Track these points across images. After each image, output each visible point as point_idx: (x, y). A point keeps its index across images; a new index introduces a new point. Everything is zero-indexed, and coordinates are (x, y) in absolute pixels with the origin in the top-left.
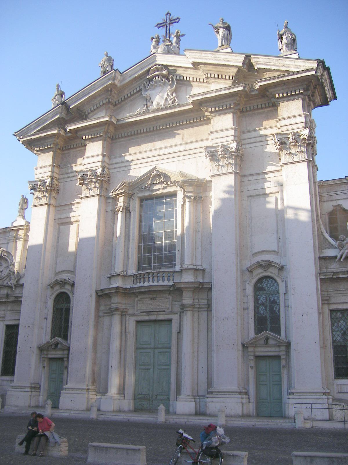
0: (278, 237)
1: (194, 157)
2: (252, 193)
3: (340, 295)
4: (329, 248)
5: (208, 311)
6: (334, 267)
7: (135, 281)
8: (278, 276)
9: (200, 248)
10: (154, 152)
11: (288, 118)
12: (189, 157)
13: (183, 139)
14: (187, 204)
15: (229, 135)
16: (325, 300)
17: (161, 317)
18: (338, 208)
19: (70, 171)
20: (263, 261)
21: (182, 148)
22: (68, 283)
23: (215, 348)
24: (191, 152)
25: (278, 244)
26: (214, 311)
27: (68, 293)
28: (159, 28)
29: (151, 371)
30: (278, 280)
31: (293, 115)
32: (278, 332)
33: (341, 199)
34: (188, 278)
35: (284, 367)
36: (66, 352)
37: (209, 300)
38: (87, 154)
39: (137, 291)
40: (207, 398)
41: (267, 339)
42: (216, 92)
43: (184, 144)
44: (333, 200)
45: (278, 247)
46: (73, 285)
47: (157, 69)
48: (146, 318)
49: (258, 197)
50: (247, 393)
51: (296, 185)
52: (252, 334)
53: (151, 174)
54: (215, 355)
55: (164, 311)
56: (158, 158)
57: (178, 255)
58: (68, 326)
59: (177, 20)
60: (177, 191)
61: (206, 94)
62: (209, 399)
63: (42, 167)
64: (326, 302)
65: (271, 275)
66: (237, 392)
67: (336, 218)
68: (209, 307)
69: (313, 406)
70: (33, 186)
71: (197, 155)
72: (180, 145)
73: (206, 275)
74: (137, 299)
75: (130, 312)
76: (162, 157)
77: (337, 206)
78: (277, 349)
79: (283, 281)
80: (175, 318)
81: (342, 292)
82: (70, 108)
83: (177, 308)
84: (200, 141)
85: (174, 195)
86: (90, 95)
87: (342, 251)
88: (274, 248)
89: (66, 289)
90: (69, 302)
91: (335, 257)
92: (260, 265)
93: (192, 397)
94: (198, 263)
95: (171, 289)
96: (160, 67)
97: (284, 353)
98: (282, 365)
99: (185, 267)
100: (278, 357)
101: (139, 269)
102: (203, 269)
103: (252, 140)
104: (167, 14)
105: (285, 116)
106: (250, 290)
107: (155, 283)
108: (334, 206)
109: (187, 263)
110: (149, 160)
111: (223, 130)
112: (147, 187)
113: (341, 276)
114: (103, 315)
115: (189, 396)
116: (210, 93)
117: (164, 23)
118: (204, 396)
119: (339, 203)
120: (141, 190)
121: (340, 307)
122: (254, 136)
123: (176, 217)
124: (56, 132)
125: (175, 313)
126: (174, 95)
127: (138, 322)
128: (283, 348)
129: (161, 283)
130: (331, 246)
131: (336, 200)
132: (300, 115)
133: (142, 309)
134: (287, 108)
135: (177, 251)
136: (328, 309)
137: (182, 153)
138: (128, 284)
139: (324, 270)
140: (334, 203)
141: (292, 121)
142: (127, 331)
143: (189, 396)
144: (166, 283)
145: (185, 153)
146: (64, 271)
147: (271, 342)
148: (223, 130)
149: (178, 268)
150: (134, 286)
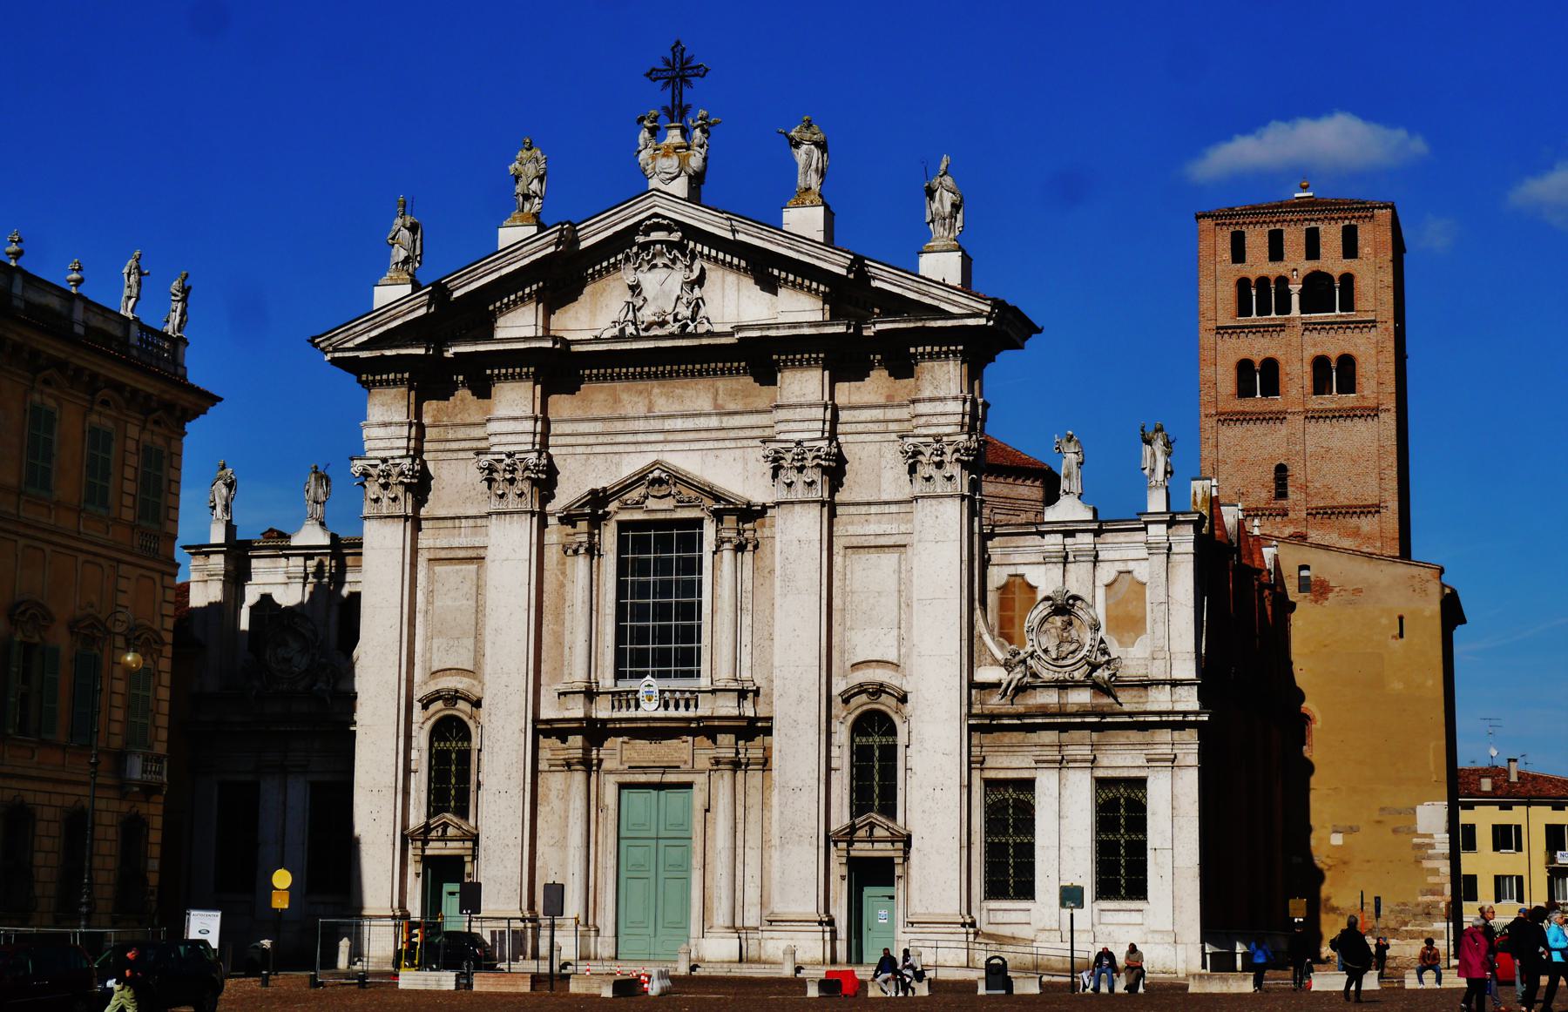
0: (899, 636)
1: (739, 445)
2: (855, 542)
3: (1003, 753)
4: (992, 665)
5: (764, 771)
6: (995, 702)
7: (616, 704)
8: (897, 713)
9: (749, 646)
10: (652, 421)
11: (931, 400)
12: (728, 444)
13: (715, 399)
14: (727, 555)
15: (813, 417)
16: (974, 763)
17: (671, 778)
18: (1018, 580)
19: (450, 437)
20: (871, 684)
21: (714, 422)
22: (466, 699)
23: (776, 841)
24: (732, 434)
25: (899, 650)
26: (775, 773)
27: (466, 718)
28: (654, 80)
29: (653, 880)
30: (897, 719)
31: (942, 394)
32: (892, 815)
33: (1024, 564)
34: (727, 707)
35: (899, 877)
36: (469, 844)
37: (767, 750)
38: (500, 411)
39: (623, 725)
40: (762, 931)
41: (872, 826)
42: (789, 328)
43: (717, 414)
44: (1010, 565)
45: (899, 655)
46: (477, 704)
47: (658, 227)
48: (642, 778)
49: (866, 549)
50: (831, 922)
51: (937, 542)
52: (841, 818)
53: (646, 475)
54: (776, 855)
55: (678, 767)
56: (661, 437)
57: (705, 656)
58: (469, 788)
59: (701, 72)
60: (702, 519)
61: (769, 329)
62: (766, 934)
63: (385, 425)
64: (978, 766)
65: (883, 708)
66: (815, 921)
67: (1013, 599)
68: (765, 764)
69: (940, 944)
70: (364, 469)
71: (745, 443)
72: (709, 415)
73: (761, 698)
74: (621, 739)
75: (606, 765)
76: (670, 437)
77: (1016, 575)
78: (889, 846)
79: (905, 722)
80: (700, 780)
81: (1006, 749)
82: (457, 294)
83: (703, 761)
84: (751, 412)
85: (698, 523)
86: (504, 272)
87: (1011, 675)
88: (892, 657)
89: (456, 709)
90: (467, 736)
91: (998, 685)
92: (861, 689)
93: (733, 931)
94: (746, 674)
95: (693, 725)
96: (665, 222)
97: (901, 854)
98: (896, 874)
99: (720, 685)
100: (888, 863)
101: (619, 675)
102: (755, 688)
103: (860, 428)
104: (673, 49)
105: (927, 394)
106: (842, 735)
107: (661, 713)
108: (1011, 576)
109: (724, 675)
110: (640, 438)
111: (801, 406)
112: (638, 503)
113: (1006, 722)
114: (547, 768)
115: (728, 928)
116: (778, 328)
117: (664, 71)
118: (757, 929)
119: (1020, 570)
120: (625, 507)
121: (1001, 775)
122: (862, 418)
123: (700, 573)
124: (422, 351)
125: (701, 772)
126: (697, 292)
127: (622, 786)
128: (900, 845)
129: (671, 712)
130: (995, 662)
131: (1014, 564)
132: (955, 398)
133: (630, 762)
134: (932, 376)
135: (702, 645)
136: (981, 778)
137: (714, 435)
138: (602, 710)
139: (976, 709)
140: (1012, 570)
141: (939, 407)
142: (601, 804)
143: (728, 928)
144: (682, 713)
145: (721, 434)
146: (450, 669)
147: (878, 832)
148: (801, 406)
149: (704, 683)
150: (616, 715)
